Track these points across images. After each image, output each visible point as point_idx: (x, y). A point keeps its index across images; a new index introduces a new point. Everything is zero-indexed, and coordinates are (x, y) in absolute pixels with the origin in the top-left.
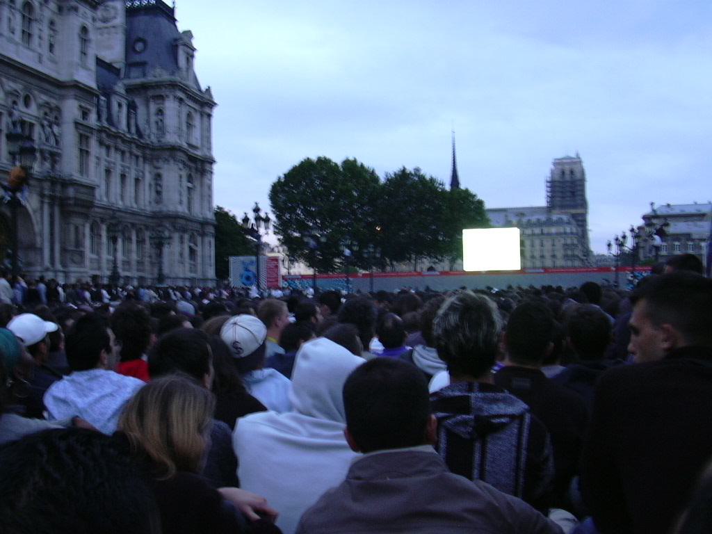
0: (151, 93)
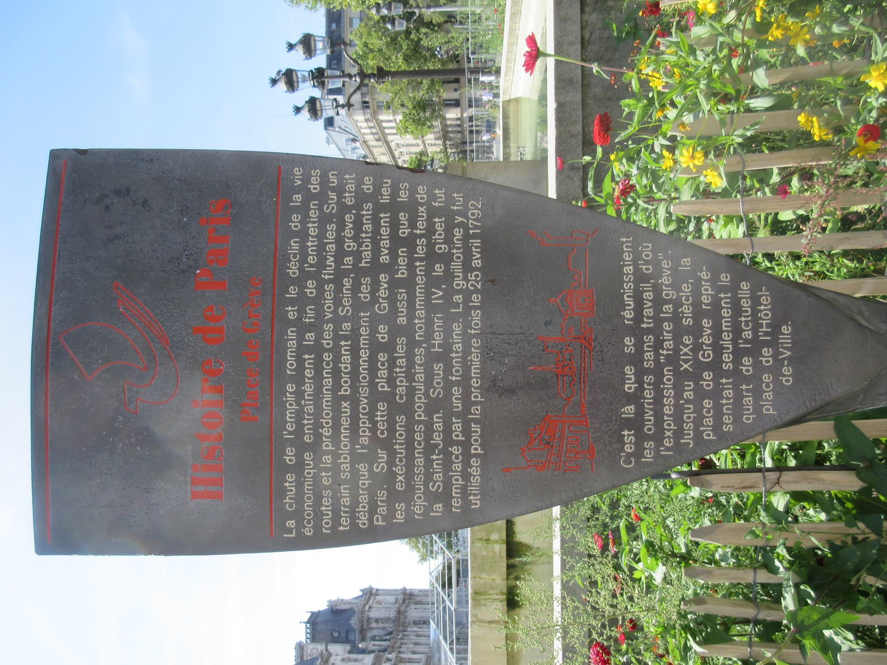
0: (365, 627)
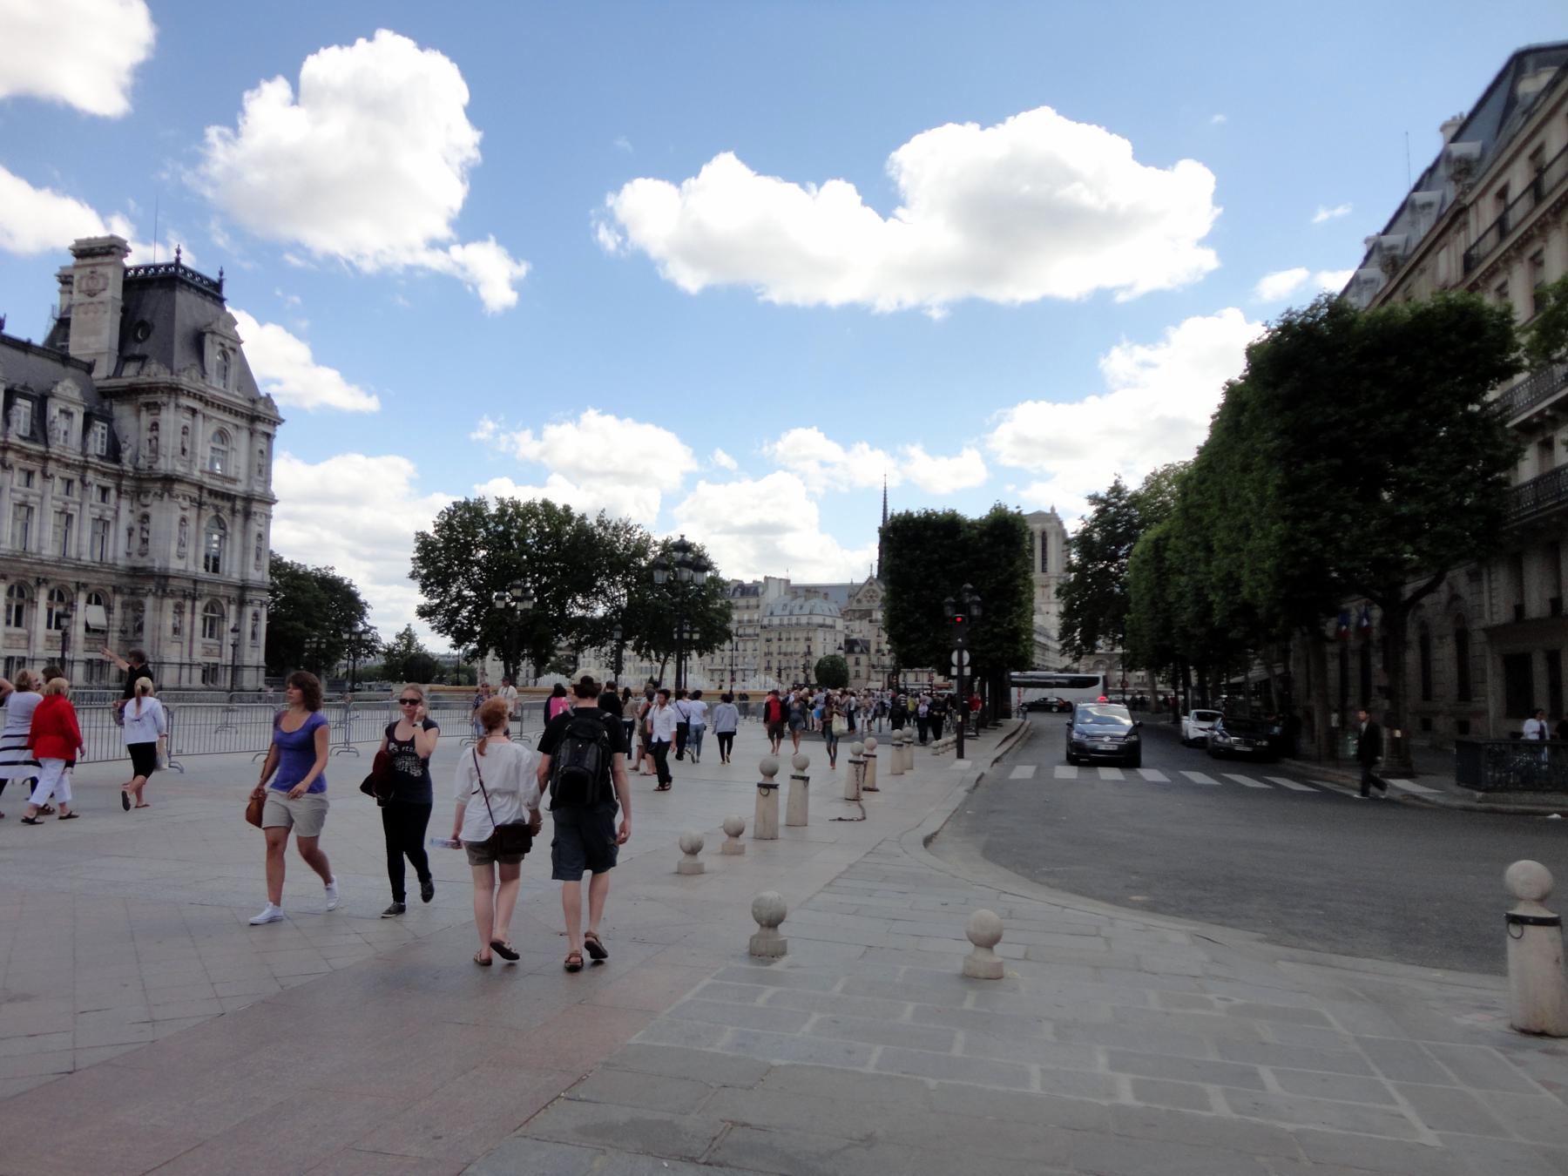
0: (143, 399)
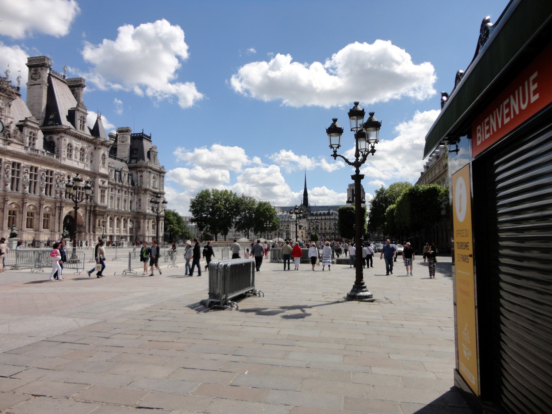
0: (138, 169)
